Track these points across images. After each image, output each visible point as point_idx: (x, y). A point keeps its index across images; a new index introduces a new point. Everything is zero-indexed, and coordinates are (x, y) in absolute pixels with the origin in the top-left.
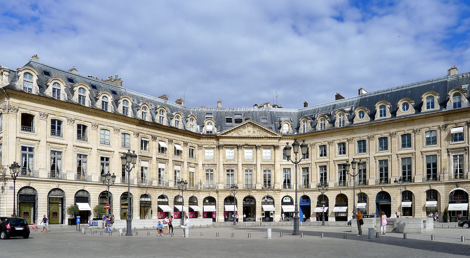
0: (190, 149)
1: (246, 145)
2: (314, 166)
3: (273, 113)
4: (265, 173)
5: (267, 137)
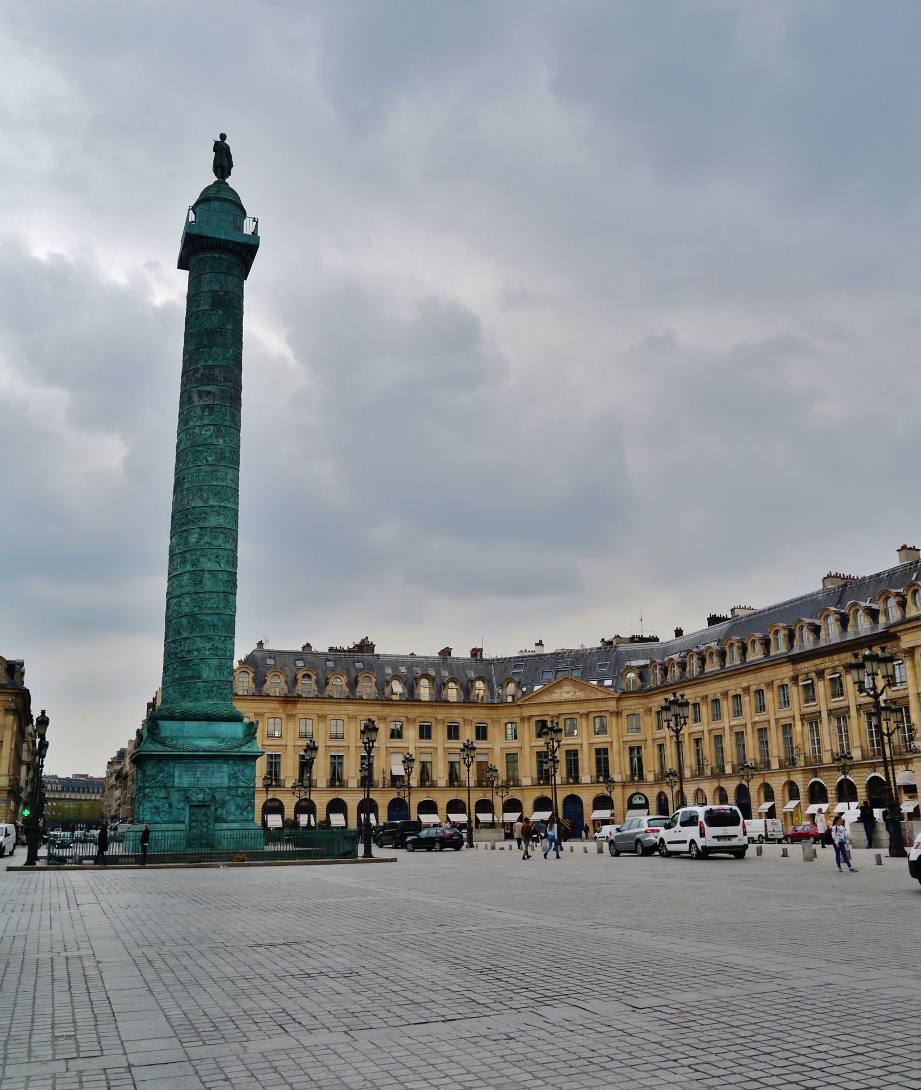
2: (668, 743)
3: (622, 653)
4: (598, 756)
5: (595, 699)
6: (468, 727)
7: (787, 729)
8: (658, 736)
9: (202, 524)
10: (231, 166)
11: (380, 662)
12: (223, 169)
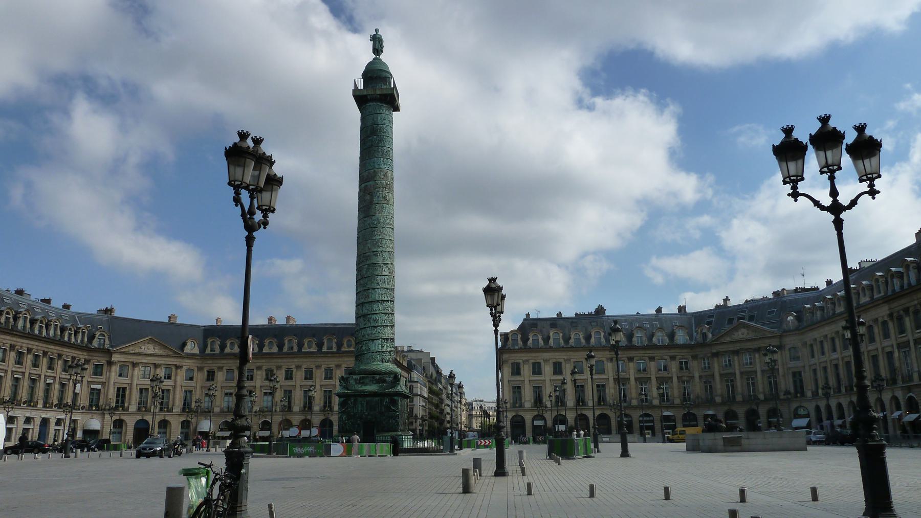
0: (681, 363)
1: (742, 349)
5: (763, 337)
6: (673, 362)
7: (890, 355)
8: (812, 363)
9: (368, 263)
10: (382, 48)
11: (609, 321)
12: (377, 51)
